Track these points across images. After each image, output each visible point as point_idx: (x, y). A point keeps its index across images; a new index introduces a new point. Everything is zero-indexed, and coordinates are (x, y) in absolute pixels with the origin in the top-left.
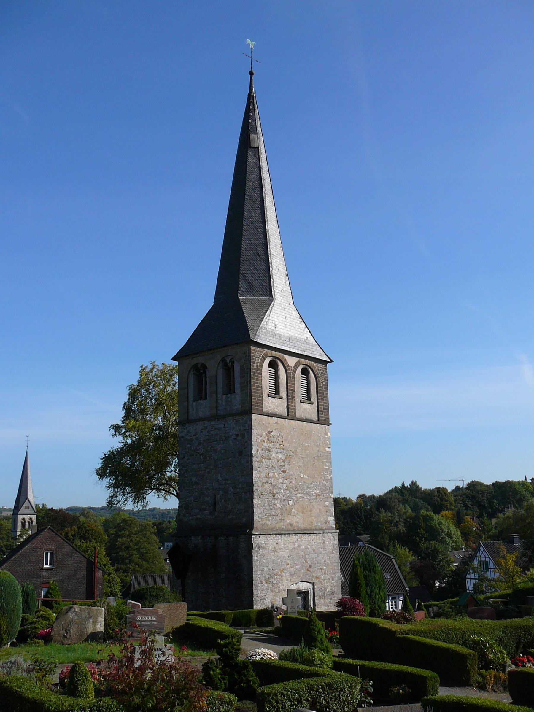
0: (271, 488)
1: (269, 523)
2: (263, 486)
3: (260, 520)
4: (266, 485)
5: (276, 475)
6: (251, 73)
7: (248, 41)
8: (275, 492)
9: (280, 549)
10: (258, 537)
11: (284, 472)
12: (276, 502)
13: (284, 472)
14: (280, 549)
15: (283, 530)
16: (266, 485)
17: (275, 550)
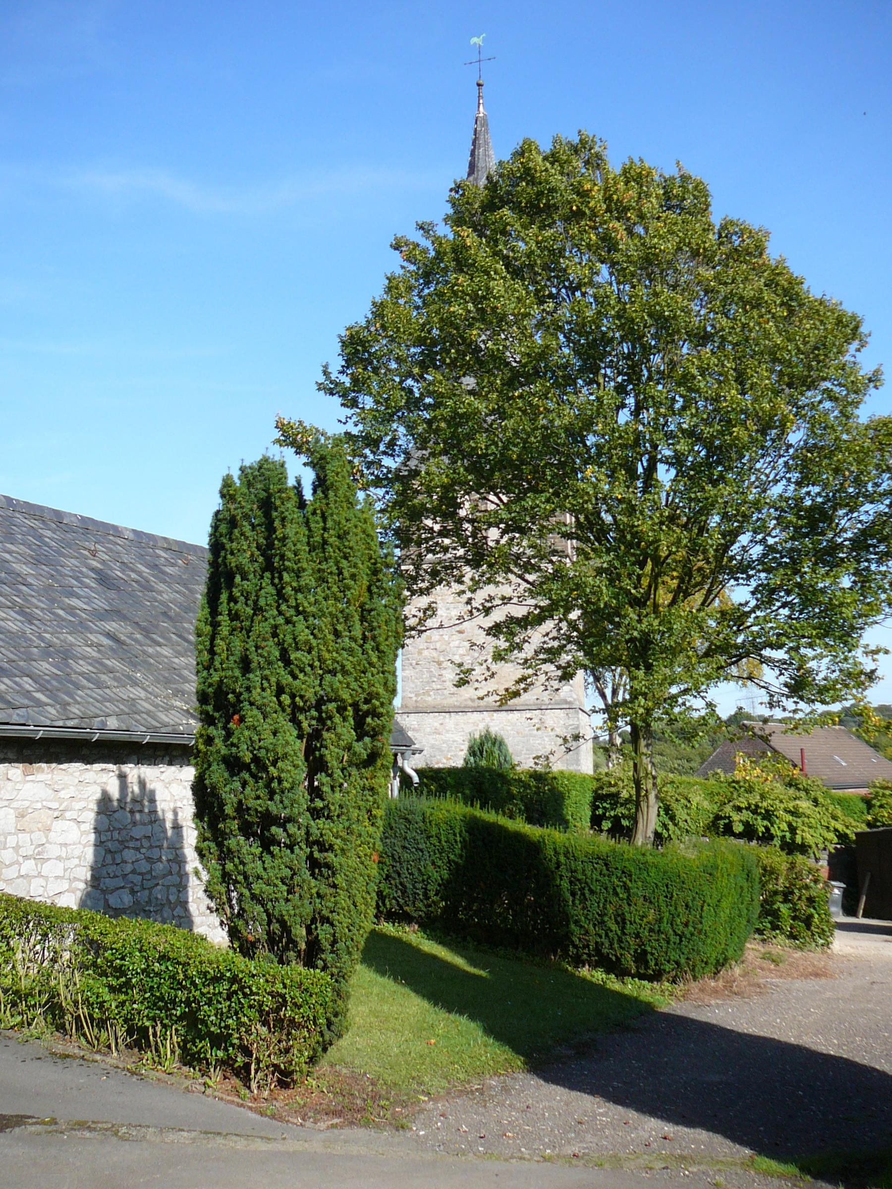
0: (434, 654)
1: (429, 699)
2: (420, 653)
3: (412, 695)
4: (426, 653)
5: (446, 637)
6: (479, 85)
7: (475, 40)
8: (442, 659)
9: (447, 731)
10: (405, 716)
11: (460, 632)
12: (444, 672)
13: (460, 632)
14: (447, 731)
15: (455, 706)
16: (426, 653)
17: (436, 732)
